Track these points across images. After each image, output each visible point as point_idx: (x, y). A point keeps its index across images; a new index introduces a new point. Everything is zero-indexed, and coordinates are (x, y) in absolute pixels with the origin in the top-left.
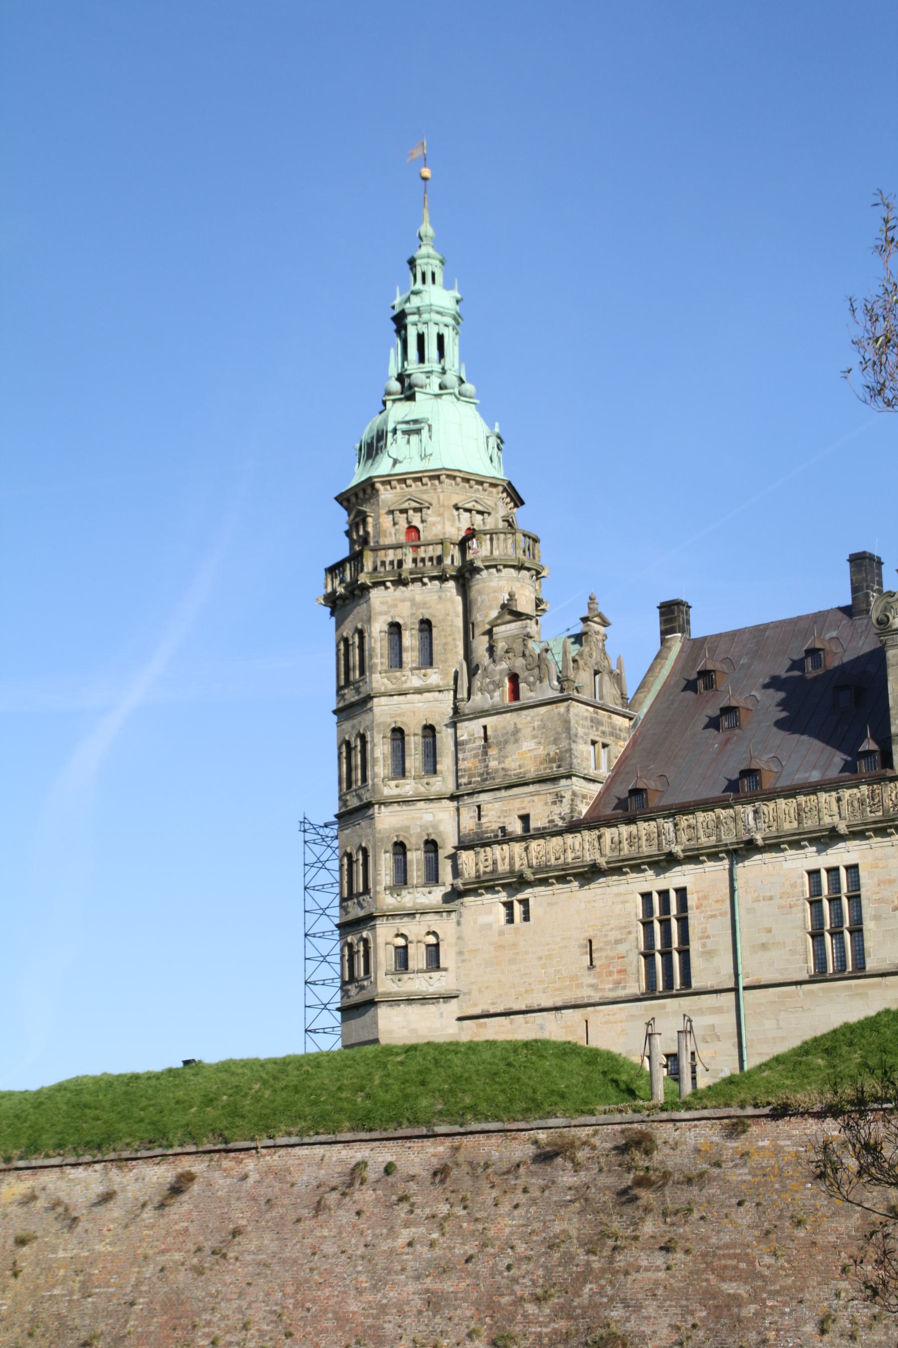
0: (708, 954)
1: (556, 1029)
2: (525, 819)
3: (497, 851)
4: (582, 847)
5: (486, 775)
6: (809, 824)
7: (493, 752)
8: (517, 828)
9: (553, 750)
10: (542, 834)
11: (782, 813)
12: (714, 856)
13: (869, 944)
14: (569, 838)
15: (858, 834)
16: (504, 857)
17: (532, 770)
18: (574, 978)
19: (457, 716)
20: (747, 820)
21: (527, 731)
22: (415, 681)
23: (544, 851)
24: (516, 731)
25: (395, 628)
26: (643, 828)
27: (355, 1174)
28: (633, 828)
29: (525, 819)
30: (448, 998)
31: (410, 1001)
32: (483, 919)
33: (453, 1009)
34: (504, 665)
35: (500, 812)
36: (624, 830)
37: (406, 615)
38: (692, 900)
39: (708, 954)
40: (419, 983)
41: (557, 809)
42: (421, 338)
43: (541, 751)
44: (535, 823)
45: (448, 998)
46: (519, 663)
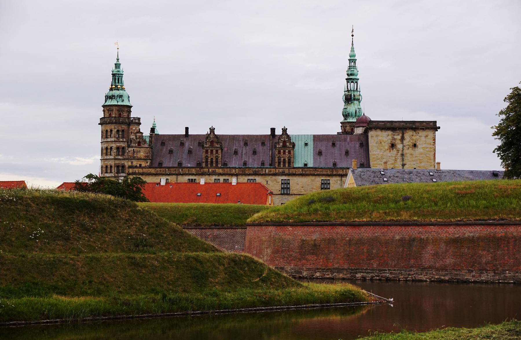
2: (140, 165)
4: (152, 171)
8: (138, 166)
16: (137, 170)
17: (142, 157)
22: (121, 140)
23: (145, 170)
25: (118, 131)
28: (161, 169)
29: (140, 165)
37: (120, 128)
42: (118, 79)
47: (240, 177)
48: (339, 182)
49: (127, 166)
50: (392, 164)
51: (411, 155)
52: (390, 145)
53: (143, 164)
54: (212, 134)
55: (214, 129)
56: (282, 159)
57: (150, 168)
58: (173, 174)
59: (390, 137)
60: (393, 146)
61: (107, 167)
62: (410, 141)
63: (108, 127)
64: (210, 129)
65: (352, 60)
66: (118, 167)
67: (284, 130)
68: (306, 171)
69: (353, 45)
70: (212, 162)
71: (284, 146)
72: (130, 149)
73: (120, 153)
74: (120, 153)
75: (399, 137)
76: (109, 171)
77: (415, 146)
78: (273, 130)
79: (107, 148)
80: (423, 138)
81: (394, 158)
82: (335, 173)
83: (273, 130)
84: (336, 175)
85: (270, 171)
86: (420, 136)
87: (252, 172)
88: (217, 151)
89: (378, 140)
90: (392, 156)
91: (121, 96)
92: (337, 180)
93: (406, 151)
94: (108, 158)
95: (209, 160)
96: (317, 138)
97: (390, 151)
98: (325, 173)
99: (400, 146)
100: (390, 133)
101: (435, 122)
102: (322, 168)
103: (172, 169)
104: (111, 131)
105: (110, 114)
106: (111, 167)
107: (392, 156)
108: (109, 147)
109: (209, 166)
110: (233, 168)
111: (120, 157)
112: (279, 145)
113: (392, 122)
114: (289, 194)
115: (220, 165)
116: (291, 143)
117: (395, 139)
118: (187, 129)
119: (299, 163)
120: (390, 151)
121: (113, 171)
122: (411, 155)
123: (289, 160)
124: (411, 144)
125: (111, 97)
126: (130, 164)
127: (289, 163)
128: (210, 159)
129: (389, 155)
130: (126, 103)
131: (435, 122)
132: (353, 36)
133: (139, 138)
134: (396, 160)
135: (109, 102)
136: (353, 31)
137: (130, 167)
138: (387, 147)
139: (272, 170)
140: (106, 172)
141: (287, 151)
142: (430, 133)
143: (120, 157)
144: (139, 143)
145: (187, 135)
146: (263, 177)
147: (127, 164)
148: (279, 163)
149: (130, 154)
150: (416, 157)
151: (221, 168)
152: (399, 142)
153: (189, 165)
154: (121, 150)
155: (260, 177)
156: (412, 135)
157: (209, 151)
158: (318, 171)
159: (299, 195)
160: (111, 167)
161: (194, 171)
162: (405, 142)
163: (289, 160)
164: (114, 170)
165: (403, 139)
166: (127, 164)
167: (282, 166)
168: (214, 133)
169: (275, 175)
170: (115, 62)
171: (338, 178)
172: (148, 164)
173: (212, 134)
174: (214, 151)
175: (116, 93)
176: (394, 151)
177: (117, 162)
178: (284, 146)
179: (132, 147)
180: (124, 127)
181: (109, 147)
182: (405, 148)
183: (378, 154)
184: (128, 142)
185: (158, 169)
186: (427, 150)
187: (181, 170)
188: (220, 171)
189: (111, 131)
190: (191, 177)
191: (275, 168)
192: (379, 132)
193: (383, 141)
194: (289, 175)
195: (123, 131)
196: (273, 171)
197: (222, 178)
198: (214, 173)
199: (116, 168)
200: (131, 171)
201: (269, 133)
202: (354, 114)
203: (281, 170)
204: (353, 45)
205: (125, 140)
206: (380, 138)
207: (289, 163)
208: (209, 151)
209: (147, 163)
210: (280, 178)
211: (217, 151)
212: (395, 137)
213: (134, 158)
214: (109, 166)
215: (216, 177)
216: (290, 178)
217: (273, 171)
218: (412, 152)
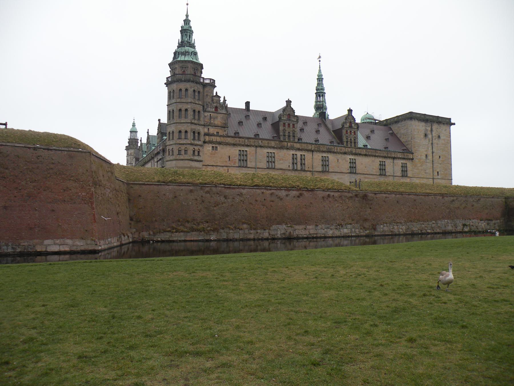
0: (251, 162)
1: (222, 170)
5: (210, 123)
7: (212, 119)
8: (215, 134)
10: (221, 136)
13: (276, 164)
15: (276, 148)
16: (214, 139)
17: (220, 124)
18: (226, 162)
21: (219, 118)
24: (217, 117)
25: (194, 91)
27: (329, 196)
28: (240, 139)
30: (201, 161)
31: (195, 161)
32: (208, 148)
33: (201, 163)
34: (215, 104)
35: (212, 130)
37: (196, 89)
38: (248, 153)
39: (251, 162)
40: (196, 158)
44: (220, 134)
45: (201, 161)
47: (315, 153)
48: (392, 164)
50: (426, 151)
55: (291, 102)
56: (349, 139)
58: (253, 146)
59: (424, 128)
60: (426, 135)
63: (183, 86)
64: (286, 101)
65: (320, 79)
66: (194, 132)
68: (367, 152)
69: (320, 67)
70: (289, 136)
71: (351, 127)
72: (206, 114)
73: (197, 117)
74: (197, 117)
75: (429, 129)
76: (183, 136)
77: (439, 137)
79: (180, 110)
82: (389, 155)
84: (389, 157)
85: (341, 150)
87: (325, 150)
88: (293, 125)
93: (434, 141)
94: (182, 121)
95: (287, 134)
99: (430, 136)
100: (423, 124)
101: (450, 119)
102: (380, 150)
104: (186, 90)
106: (186, 132)
108: (183, 109)
109: (287, 140)
110: (310, 143)
111: (196, 122)
113: (425, 115)
114: (355, 173)
117: (426, 130)
118: (248, 104)
123: (355, 140)
125: (185, 54)
126: (206, 130)
127: (355, 143)
128: (287, 132)
131: (450, 119)
132: (320, 61)
133: (216, 102)
135: (181, 58)
136: (320, 57)
137: (205, 134)
141: (353, 132)
144: (216, 108)
146: (335, 154)
148: (347, 142)
149: (207, 120)
154: (197, 113)
155: (332, 154)
157: (287, 124)
159: (363, 174)
160: (186, 132)
161: (273, 144)
162: (433, 133)
164: (190, 135)
165: (432, 130)
166: (203, 130)
169: (345, 153)
170: (185, 18)
171: (391, 160)
174: (291, 125)
178: (351, 127)
179: (209, 112)
181: (183, 109)
184: (203, 106)
185: (238, 139)
187: (260, 142)
188: (298, 146)
189: (186, 90)
190: (270, 150)
191: (344, 147)
194: (356, 154)
197: (299, 153)
198: (292, 148)
199: (192, 133)
200: (207, 138)
203: (349, 149)
204: (320, 67)
205: (200, 103)
207: (355, 143)
208: (287, 124)
211: (293, 125)
213: (210, 125)
214: (183, 131)
217: (344, 150)
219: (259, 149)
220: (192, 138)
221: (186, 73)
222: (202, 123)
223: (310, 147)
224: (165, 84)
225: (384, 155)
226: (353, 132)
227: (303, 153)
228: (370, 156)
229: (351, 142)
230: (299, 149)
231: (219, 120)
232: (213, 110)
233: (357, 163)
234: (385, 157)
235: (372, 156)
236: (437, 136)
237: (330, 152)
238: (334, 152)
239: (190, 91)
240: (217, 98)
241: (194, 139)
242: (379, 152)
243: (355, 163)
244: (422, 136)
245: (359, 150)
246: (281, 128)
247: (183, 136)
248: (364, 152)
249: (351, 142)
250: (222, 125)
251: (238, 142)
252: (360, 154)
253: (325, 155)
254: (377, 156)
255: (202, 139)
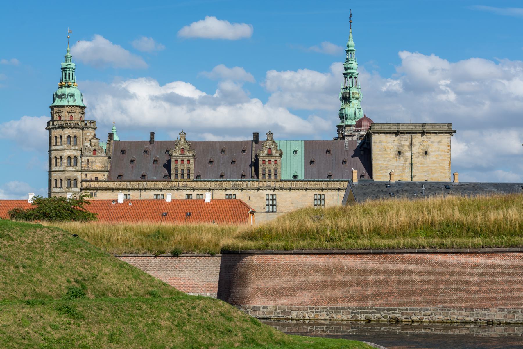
2: (96, 178)
3: (91, 183)
4: (111, 185)
5: (88, 168)
6: (156, 187)
7: (90, 164)
8: (94, 179)
9: (103, 166)
10: (101, 181)
11: (151, 184)
12: (137, 190)
14: (107, 183)
16: (92, 184)
17: (99, 169)
19: (82, 156)
20: (144, 184)
21: (97, 161)
22: (73, 148)
25: (69, 136)
26: (122, 183)
29: (96, 178)
34: (93, 148)
36: (119, 183)
37: (72, 135)
41: (104, 177)
42: (69, 74)
43: (101, 165)
46: (97, 148)
49: (80, 180)
50: (399, 175)
51: (422, 164)
52: (397, 153)
53: (100, 177)
54: (183, 140)
57: (108, 181)
58: (137, 190)
59: (396, 143)
60: (399, 153)
61: (56, 180)
62: (420, 148)
67: (270, 134)
68: (294, 185)
70: (183, 174)
71: (270, 154)
72: (83, 159)
73: (72, 164)
74: (72, 164)
75: (407, 143)
76: (59, 185)
77: (426, 153)
78: (256, 135)
80: (436, 144)
81: (401, 168)
83: (256, 135)
84: (330, 189)
86: (432, 142)
88: (189, 160)
89: (383, 146)
90: (399, 166)
91: (72, 95)
92: (333, 195)
93: (415, 160)
94: (57, 169)
95: (180, 172)
96: (309, 145)
97: (397, 160)
98: (318, 187)
99: (408, 154)
103: (135, 183)
105: (59, 116)
107: (399, 166)
108: (58, 157)
112: (263, 152)
115: (192, 178)
116: (277, 150)
117: (402, 146)
118: (152, 134)
119: (286, 174)
120: (397, 160)
121: (63, 186)
122: (422, 164)
123: (276, 170)
124: (422, 151)
125: (61, 96)
126: (84, 176)
127: (276, 174)
129: (396, 164)
130: (78, 103)
131: (449, 125)
134: (403, 171)
136: (351, 17)
137: (83, 181)
138: (392, 156)
139: (256, 183)
140: (56, 187)
142: (444, 138)
143: (71, 169)
145: (152, 141)
147: (80, 176)
148: (264, 174)
149: (84, 165)
150: (428, 166)
151: (193, 181)
152: (407, 148)
153: (155, 178)
154: (72, 160)
156: (423, 141)
158: (310, 184)
161: (160, 185)
162: (413, 148)
163: (276, 170)
164: (65, 183)
165: (411, 144)
167: (267, 178)
168: (185, 139)
169: (258, 189)
171: (335, 193)
172: (106, 177)
173: (183, 140)
174: (185, 161)
175: (67, 91)
176: (402, 160)
177: (67, 174)
178: (270, 154)
179: (87, 157)
180: (76, 132)
182: (414, 156)
183: (382, 164)
186: (441, 158)
189: (61, 136)
192: (383, 137)
193: (388, 148)
194: (274, 189)
195: (75, 136)
196: (256, 184)
197: (194, 194)
198: (185, 188)
199: (66, 182)
200: (84, 185)
201: (251, 138)
202: (353, 116)
205: (77, 148)
206: (384, 144)
207: (276, 174)
208: (179, 160)
209: (104, 175)
210: (264, 193)
211: (189, 160)
212: (403, 143)
213: (88, 170)
215: (188, 192)
216: (276, 192)
217: (256, 184)
218: (424, 161)
219: (143, 192)
220: (66, 186)
221: (63, 118)
222: (79, 168)
223: (208, 185)
224: (46, 129)
225: (321, 187)
226: (273, 160)
227: (200, 192)
228: (298, 189)
229: (270, 175)
230: (194, 189)
231: (98, 164)
232: (92, 153)
233: (277, 199)
234: (322, 190)
235: (302, 189)
236: (422, 152)
237: (237, 189)
238: (242, 189)
239: (65, 137)
240: (96, 141)
241: (69, 186)
242: (312, 183)
243: (275, 200)
244: (393, 154)
245: (280, 183)
246: (173, 166)
247: (59, 185)
248: (288, 185)
249: (270, 175)
250: (101, 169)
251: (119, 187)
252: (282, 189)
253: (229, 192)
254: (310, 189)
255: (79, 185)
